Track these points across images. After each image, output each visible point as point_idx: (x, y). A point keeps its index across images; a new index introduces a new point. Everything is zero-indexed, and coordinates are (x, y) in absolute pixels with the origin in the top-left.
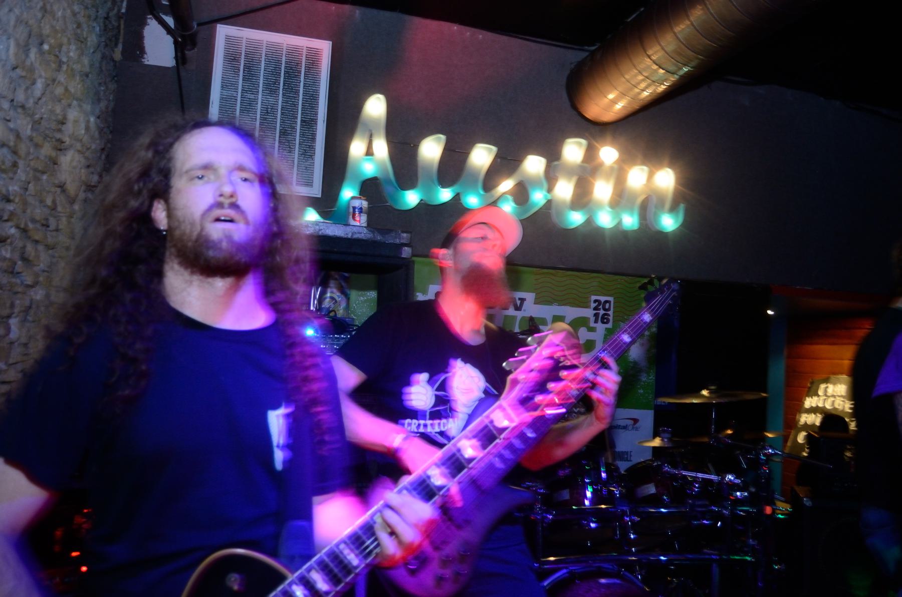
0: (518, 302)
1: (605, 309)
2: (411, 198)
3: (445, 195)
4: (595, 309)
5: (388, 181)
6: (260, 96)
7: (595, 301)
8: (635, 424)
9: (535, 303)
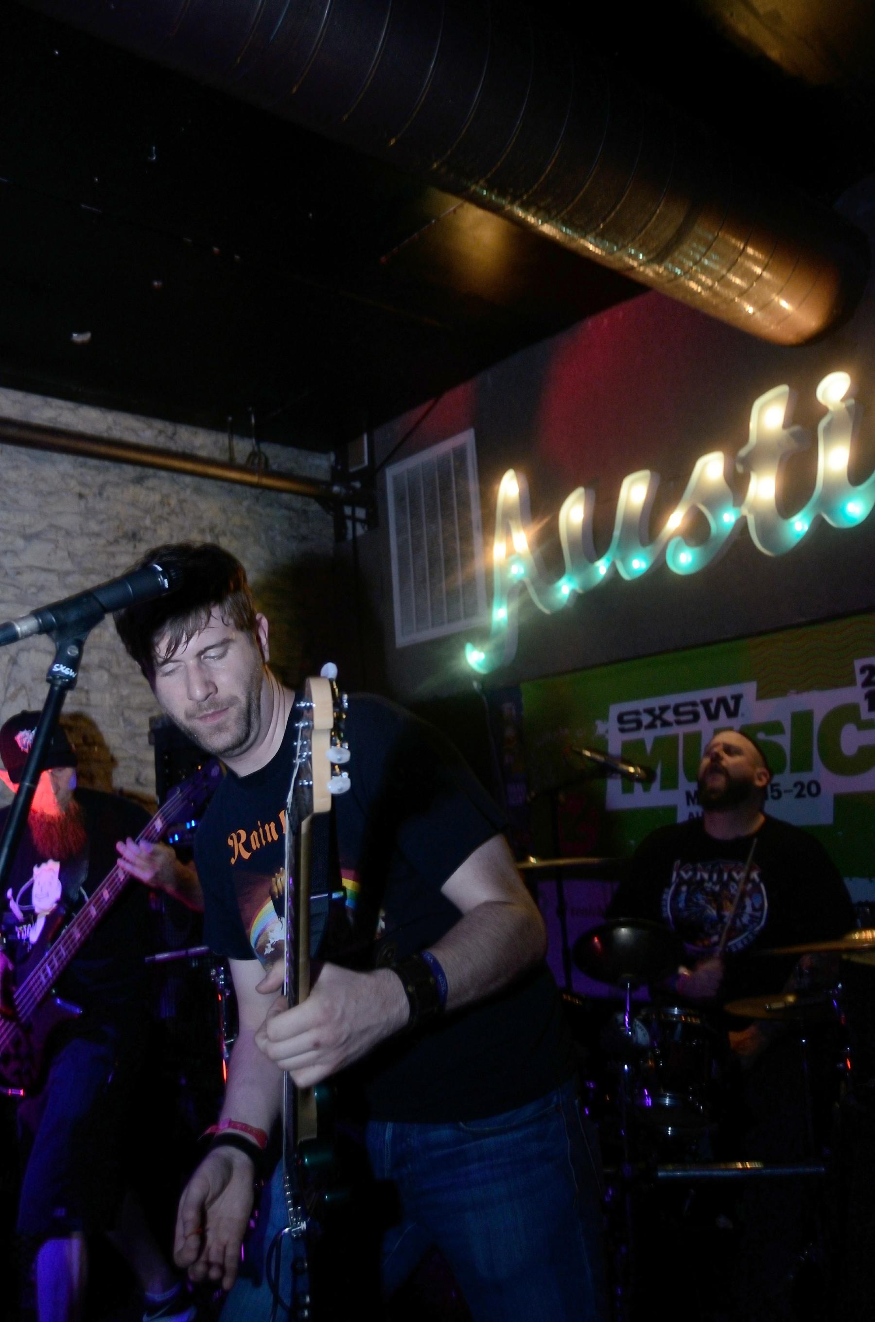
0: (732, 704)
2: (565, 589)
3: (602, 568)
6: (425, 529)
7: (863, 670)
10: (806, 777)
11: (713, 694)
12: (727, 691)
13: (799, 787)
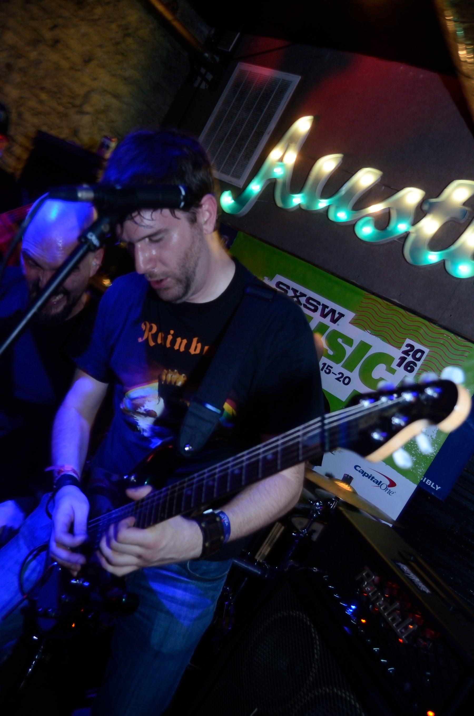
0: (337, 316)
1: (414, 356)
4: (406, 353)
5: (263, 178)
6: (240, 112)
7: (408, 345)
8: (390, 486)
9: (350, 323)
10: (346, 373)
11: (332, 305)
12: (339, 309)
13: (341, 375)
